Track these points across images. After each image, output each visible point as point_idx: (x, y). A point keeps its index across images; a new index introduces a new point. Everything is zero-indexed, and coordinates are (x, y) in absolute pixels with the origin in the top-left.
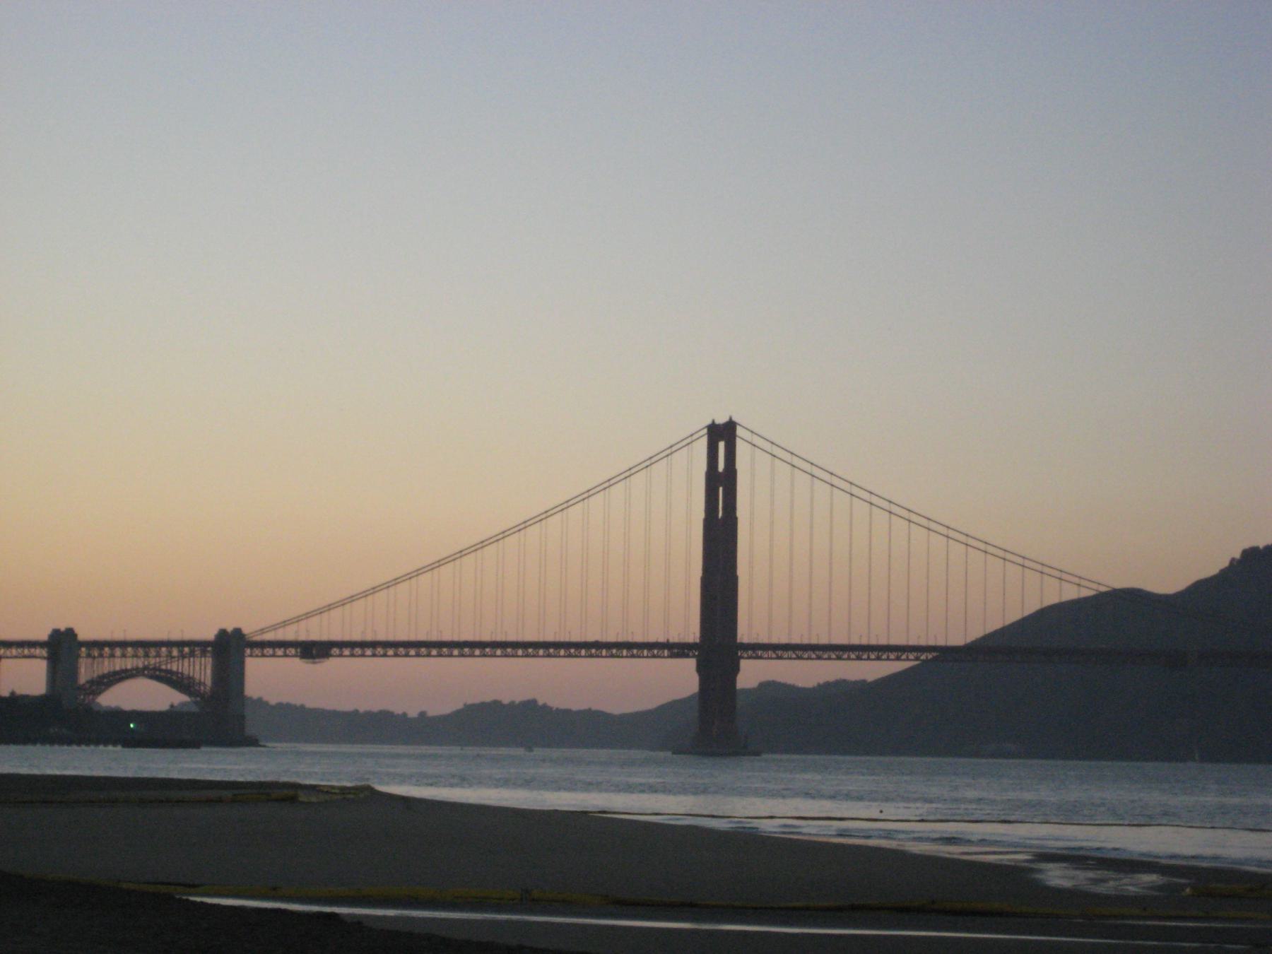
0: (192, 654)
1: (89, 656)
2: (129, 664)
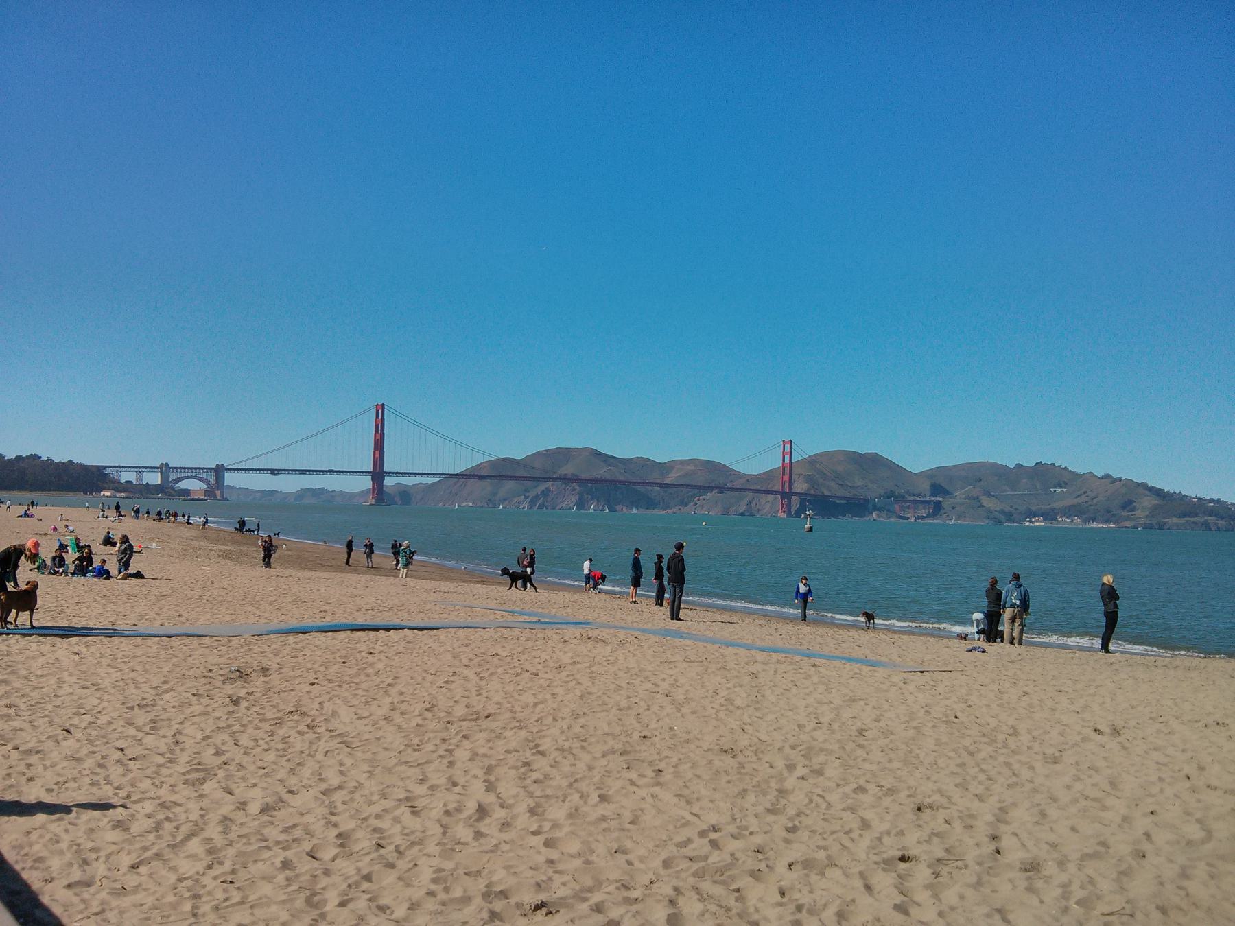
0: (207, 472)
1: (173, 472)
2: (186, 474)
